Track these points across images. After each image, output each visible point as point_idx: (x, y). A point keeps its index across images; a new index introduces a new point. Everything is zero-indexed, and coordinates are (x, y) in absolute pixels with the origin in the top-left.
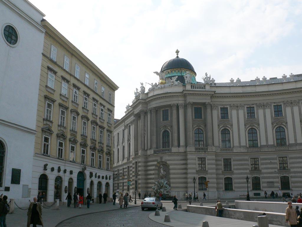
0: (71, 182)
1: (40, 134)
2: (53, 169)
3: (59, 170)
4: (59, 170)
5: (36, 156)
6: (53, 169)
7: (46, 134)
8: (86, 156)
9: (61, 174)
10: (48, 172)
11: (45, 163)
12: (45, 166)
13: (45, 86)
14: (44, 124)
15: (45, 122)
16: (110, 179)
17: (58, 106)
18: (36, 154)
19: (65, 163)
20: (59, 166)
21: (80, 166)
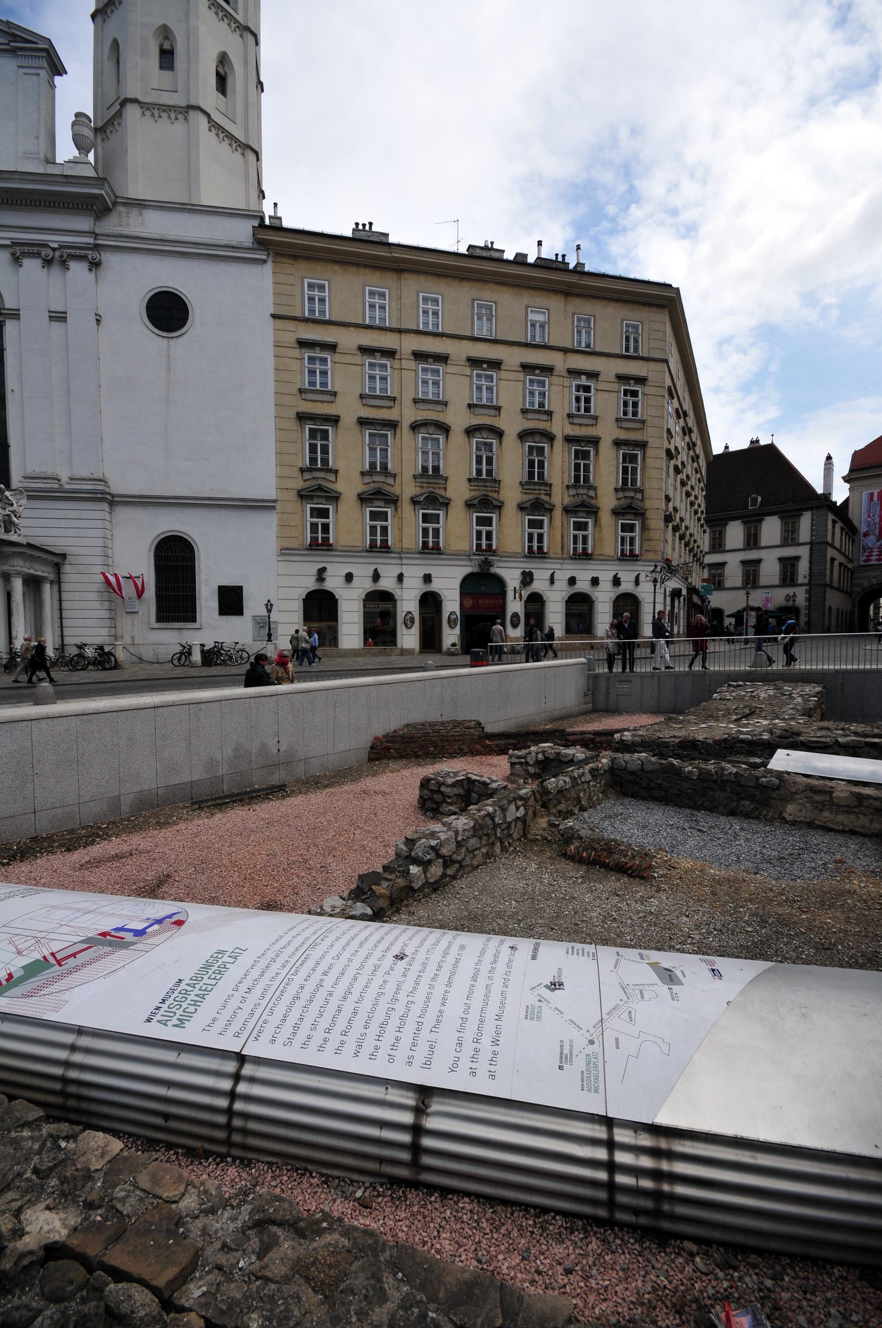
0: (430, 602)
1: (294, 506)
2: (349, 577)
3: (376, 577)
4: (376, 577)
5: (282, 554)
6: (349, 577)
7: (315, 501)
8: (498, 531)
9: (387, 584)
10: (334, 583)
11: (321, 566)
12: (322, 571)
13: (296, 392)
14: (305, 481)
15: (307, 476)
16: (637, 582)
17: (358, 428)
18: (285, 552)
19: (401, 558)
20: (375, 567)
21: (470, 560)
